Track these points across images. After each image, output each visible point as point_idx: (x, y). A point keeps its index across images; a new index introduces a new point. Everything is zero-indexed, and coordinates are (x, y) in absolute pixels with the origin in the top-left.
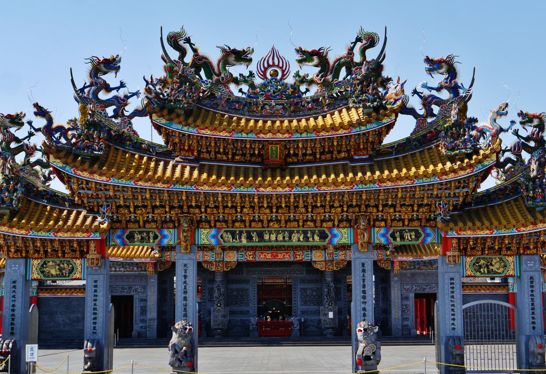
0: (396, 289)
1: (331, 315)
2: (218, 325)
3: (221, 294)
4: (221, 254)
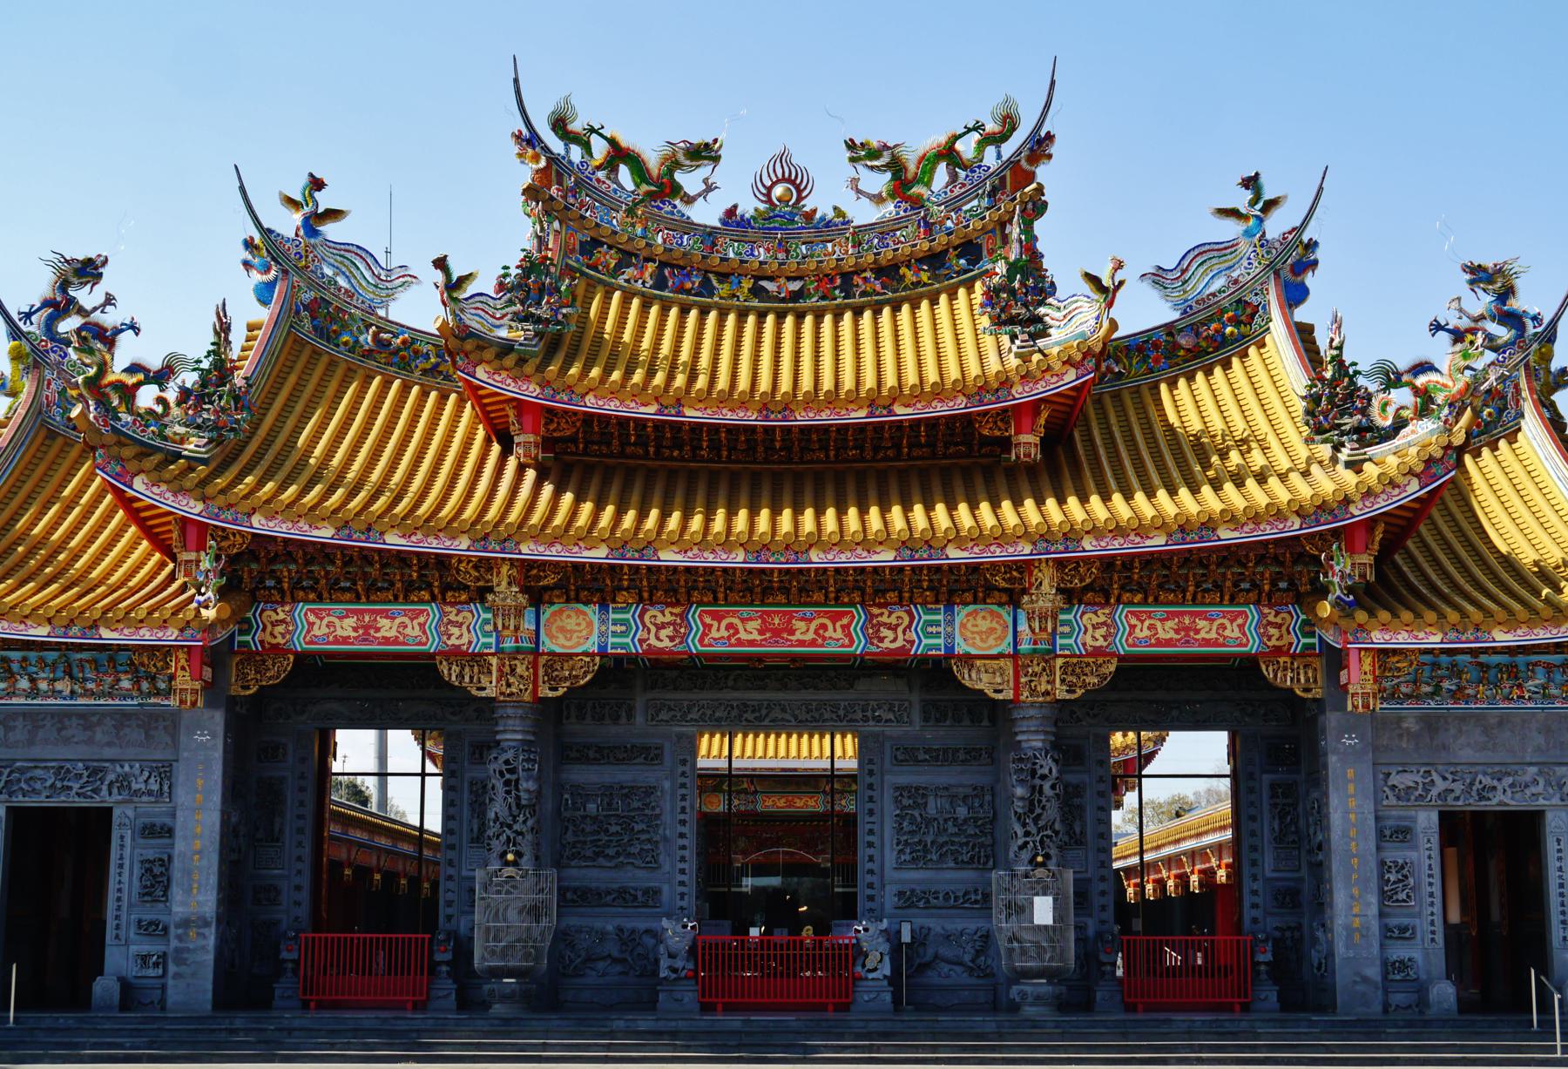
0: (1351, 788)
1: (1043, 910)
2: (504, 953)
3: (518, 805)
4: (519, 613)
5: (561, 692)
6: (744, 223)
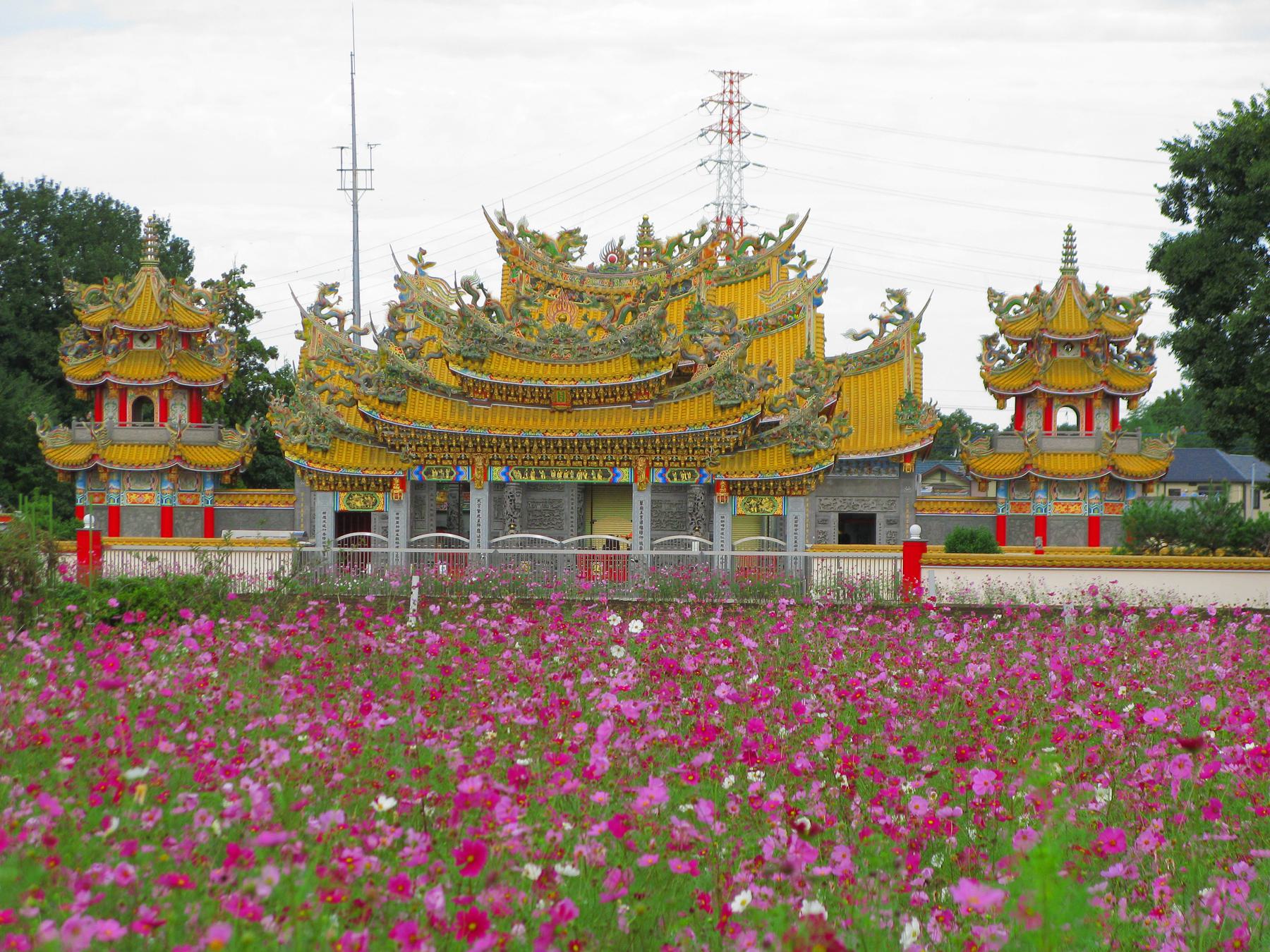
6: (596, 271)
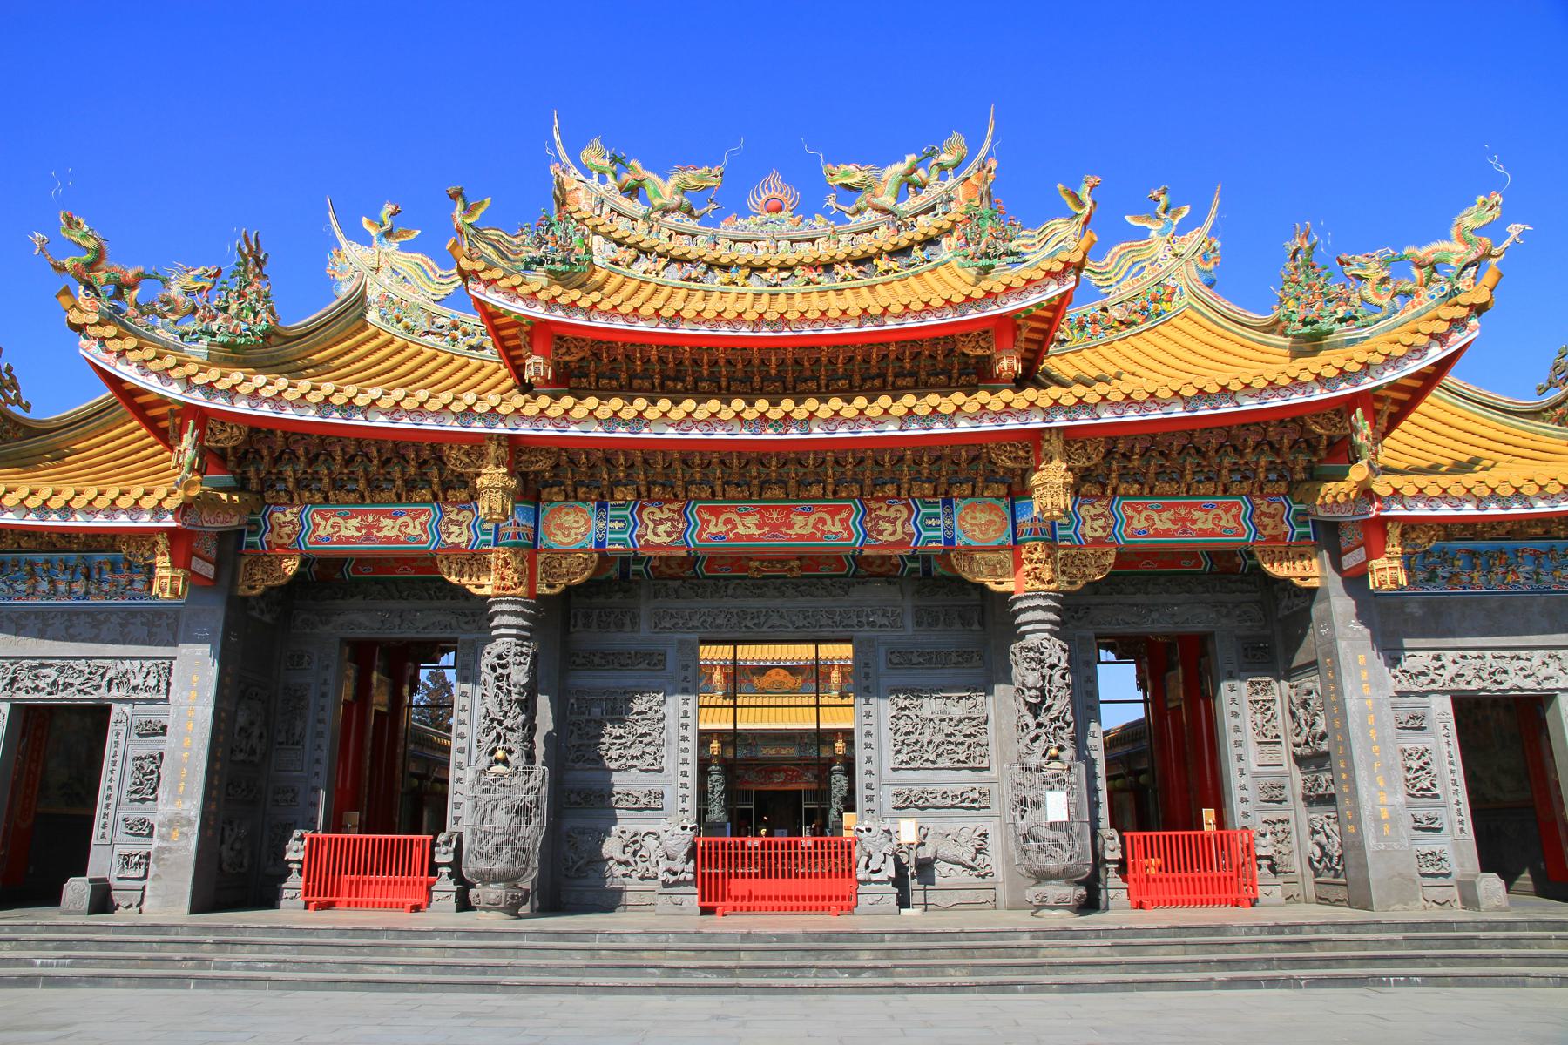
0: (1364, 675)
5: (558, 590)
